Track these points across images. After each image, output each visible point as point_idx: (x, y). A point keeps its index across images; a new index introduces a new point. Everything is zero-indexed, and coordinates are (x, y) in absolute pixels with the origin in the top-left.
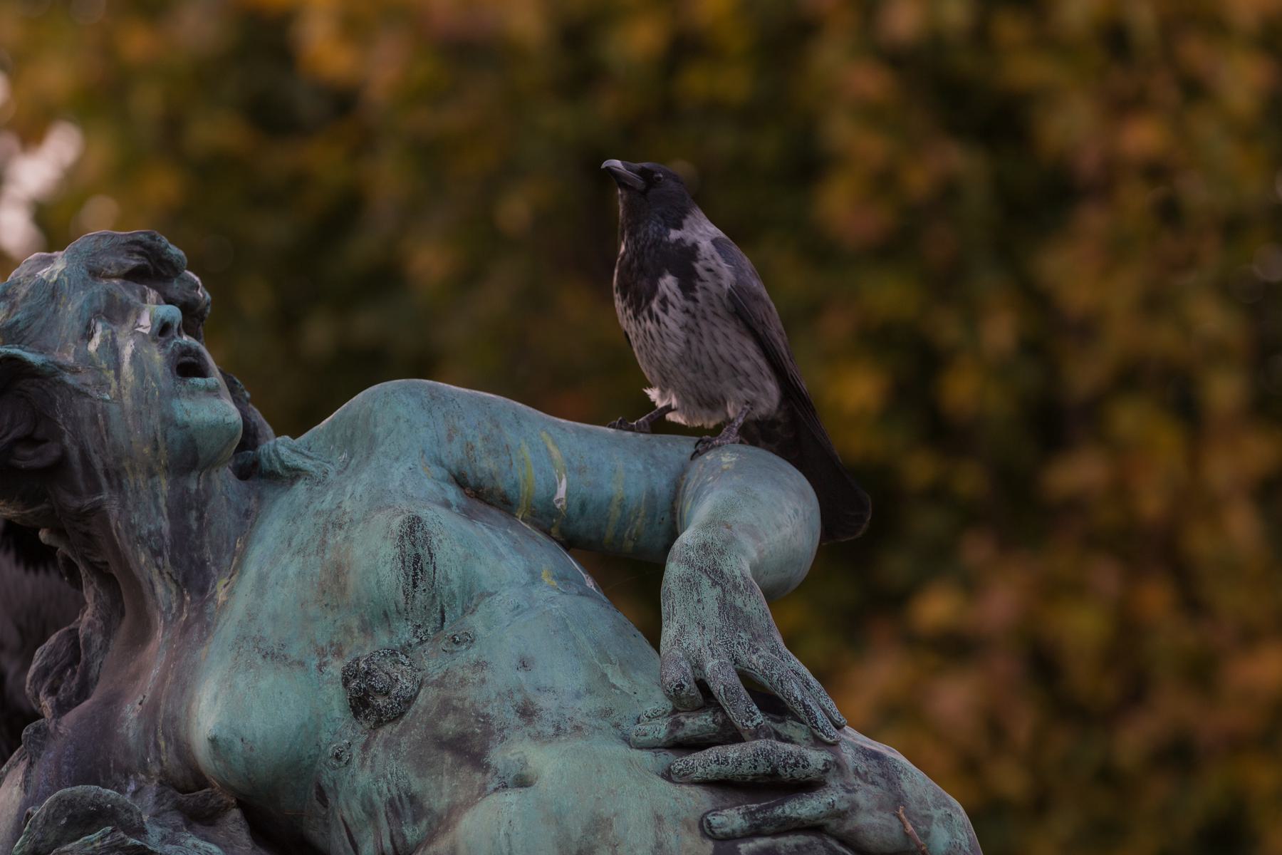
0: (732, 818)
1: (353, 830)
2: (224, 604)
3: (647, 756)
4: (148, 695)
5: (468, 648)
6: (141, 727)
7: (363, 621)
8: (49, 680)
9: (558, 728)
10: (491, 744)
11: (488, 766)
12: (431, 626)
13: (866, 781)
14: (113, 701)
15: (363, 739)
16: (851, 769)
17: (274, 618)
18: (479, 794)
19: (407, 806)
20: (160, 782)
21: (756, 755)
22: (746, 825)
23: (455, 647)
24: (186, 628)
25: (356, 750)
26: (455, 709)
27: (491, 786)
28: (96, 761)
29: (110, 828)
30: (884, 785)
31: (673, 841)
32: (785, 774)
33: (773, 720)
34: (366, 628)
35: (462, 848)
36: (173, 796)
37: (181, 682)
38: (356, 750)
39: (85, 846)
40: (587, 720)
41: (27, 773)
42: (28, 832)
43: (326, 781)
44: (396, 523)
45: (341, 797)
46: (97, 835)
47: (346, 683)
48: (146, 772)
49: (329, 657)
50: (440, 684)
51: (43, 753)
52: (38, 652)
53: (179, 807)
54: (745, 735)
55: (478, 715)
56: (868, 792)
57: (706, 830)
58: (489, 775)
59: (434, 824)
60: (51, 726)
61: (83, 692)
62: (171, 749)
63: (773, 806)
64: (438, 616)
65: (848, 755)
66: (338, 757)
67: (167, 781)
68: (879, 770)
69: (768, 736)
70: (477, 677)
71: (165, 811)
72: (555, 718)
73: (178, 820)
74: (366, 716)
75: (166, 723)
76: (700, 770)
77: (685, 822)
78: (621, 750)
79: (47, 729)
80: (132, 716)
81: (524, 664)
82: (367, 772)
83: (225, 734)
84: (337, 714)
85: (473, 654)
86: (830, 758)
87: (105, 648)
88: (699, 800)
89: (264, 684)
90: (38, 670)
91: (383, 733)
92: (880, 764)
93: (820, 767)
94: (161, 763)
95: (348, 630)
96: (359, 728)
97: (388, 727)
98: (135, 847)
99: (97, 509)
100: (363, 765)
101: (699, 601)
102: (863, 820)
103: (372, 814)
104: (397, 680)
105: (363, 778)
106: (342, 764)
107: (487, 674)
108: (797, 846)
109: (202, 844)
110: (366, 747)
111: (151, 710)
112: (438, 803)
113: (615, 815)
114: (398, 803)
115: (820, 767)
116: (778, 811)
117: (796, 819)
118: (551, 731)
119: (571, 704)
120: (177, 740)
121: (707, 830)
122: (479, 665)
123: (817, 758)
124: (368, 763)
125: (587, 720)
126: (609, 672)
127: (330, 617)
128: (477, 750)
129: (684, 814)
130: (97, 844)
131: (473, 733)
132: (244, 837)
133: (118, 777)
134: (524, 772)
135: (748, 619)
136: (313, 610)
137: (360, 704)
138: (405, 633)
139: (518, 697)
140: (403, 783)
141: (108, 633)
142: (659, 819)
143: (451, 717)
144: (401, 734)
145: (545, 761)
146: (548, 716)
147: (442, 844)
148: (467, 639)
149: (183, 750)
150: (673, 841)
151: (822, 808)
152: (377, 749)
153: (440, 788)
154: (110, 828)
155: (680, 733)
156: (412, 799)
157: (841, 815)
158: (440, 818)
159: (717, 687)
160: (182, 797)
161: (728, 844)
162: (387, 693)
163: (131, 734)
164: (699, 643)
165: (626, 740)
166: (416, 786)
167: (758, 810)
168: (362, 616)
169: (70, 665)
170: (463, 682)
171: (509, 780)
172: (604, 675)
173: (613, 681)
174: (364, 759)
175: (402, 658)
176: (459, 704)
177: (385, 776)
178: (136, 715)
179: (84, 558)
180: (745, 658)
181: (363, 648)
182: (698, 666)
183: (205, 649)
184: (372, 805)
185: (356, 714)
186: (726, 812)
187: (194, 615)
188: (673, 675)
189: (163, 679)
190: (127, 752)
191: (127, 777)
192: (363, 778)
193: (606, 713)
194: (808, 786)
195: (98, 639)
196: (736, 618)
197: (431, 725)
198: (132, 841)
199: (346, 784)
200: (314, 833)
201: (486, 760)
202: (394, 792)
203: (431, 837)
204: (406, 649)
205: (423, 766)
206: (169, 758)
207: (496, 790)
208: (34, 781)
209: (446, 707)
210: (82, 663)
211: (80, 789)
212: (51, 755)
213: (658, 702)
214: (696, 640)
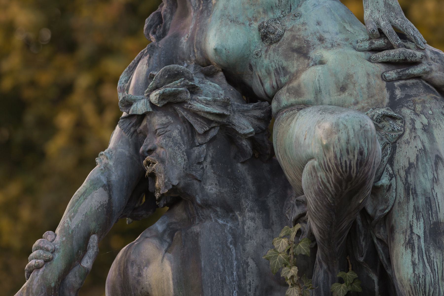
0: (392, 74)
1: (262, 79)
2: (215, 4)
3: (362, 54)
4: (190, 34)
5: (299, 18)
6: (188, 45)
7: (264, 9)
8: (152, 30)
9: (332, 45)
10: (310, 50)
11: (309, 57)
12: (287, 11)
13: (434, 61)
14: (177, 36)
15: (265, 48)
16: (430, 58)
17: (233, 8)
18: (307, 67)
19: (282, 71)
20: (195, 63)
21: (400, 53)
22: (397, 76)
23: (295, 18)
24: (202, 12)
25: (263, 52)
26: (297, 39)
27: (311, 64)
28: (172, 56)
29: (183, 79)
30: (440, 63)
31: (373, 82)
32: (409, 59)
33: (403, 41)
34: (265, 12)
35: (302, 85)
36: (200, 68)
37: (202, 29)
38: (263, 52)
39: (175, 85)
40: (341, 42)
41: (149, 60)
42: (155, 80)
43: (253, 62)
45: (258, 68)
46: (179, 81)
47: (259, 30)
48: (190, 60)
49: (253, 22)
50: (291, 30)
51: (154, 54)
52: (147, 20)
53: (202, 72)
54: (395, 47)
55: (305, 40)
56: (435, 65)
57: (383, 78)
58: (310, 60)
59: (291, 77)
60: (156, 45)
61: (164, 34)
62: (199, 52)
63: (405, 70)
64: (289, 8)
65: (429, 53)
66: (257, 55)
67: (197, 63)
68: (438, 58)
69: (402, 47)
70: (304, 28)
71: (197, 73)
72: (331, 41)
73: (202, 76)
74: (266, 41)
75: (197, 43)
76: (381, 58)
77: (377, 76)
78: (354, 52)
79: (154, 46)
80: (184, 41)
81: (318, 23)
82: (267, 60)
83: (219, 47)
84: (256, 40)
85: (302, 20)
86: (423, 54)
87: (171, 18)
88: (381, 68)
89: (232, 31)
90: (148, 26)
91: (273, 46)
92: (439, 56)
93: (420, 57)
94: (195, 57)
95: (259, 12)
96: (264, 45)
97: (274, 45)
98: (192, 85)
100: (266, 57)
101: (377, 2)
102: (434, 74)
103: (269, 73)
104: (277, 29)
105: (266, 62)
106: (258, 57)
107: (307, 27)
108: (413, 83)
109: (212, 84)
110: (267, 51)
111: (191, 39)
112: (293, 69)
113: (354, 73)
114: (278, 70)
115: (420, 57)
116: (407, 72)
117: (413, 74)
118: (330, 46)
119: (335, 37)
120: (201, 49)
121: (384, 78)
122: (304, 24)
123: (419, 54)
124: (268, 56)
125: (341, 42)
126: (346, 26)
127: (252, 8)
128: (305, 52)
129: (376, 73)
130: (179, 84)
131: (304, 46)
132: (224, 81)
133: (180, 61)
134: (322, 59)
135: (394, 8)
136: (247, 6)
137: (264, 37)
138: (278, 13)
139: (318, 34)
140: (280, 63)
141: (172, 13)
142: (368, 74)
143: (296, 41)
144: (279, 47)
145: (329, 56)
146: (328, 41)
147: (295, 84)
148: (300, 15)
149: (203, 52)
150: (373, 82)
151: (421, 71)
152: (271, 52)
153: (293, 65)
154: (183, 79)
155: (373, 46)
156: (284, 68)
157: (427, 73)
158: (293, 75)
159: (386, 31)
160: (203, 68)
161: (391, 83)
162: (274, 33)
163: (184, 47)
164: (378, 16)
165: (355, 48)
166: (285, 64)
167: (401, 71)
168: (263, 8)
169: (159, 24)
170: (299, 30)
171: (317, 62)
172: (345, 27)
173: (347, 29)
174: (266, 55)
175: (278, 22)
176: (299, 37)
177: (274, 61)
178: (186, 41)
180: (393, 21)
181: (266, 19)
182: (378, 24)
183: (209, 19)
184: (269, 70)
185: (263, 40)
186: (390, 72)
187: (204, 7)
188: (371, 26)
189: (194, 29)
190: (183, 53)
191: (183, 61)
192: (266, 62)
193: (347, 40)
194: (415, 63)
195: (168, 16)
196: (390, 8)
197: (289, 44)
198: (190, 83)
199: (260, 64)
200: (247, 80)
201: (308, 55)
202: (277, 66)
203: (290, 81)
204: (279, 19)
205: (287, 57)
206: (198, 55)
207: (313, 65)
208: (151, 63)
209: (294, 38)
210: (163, 24)
211: (172, 66)
212: (157, 54)
213: (363, 36)
214: (377, 15)
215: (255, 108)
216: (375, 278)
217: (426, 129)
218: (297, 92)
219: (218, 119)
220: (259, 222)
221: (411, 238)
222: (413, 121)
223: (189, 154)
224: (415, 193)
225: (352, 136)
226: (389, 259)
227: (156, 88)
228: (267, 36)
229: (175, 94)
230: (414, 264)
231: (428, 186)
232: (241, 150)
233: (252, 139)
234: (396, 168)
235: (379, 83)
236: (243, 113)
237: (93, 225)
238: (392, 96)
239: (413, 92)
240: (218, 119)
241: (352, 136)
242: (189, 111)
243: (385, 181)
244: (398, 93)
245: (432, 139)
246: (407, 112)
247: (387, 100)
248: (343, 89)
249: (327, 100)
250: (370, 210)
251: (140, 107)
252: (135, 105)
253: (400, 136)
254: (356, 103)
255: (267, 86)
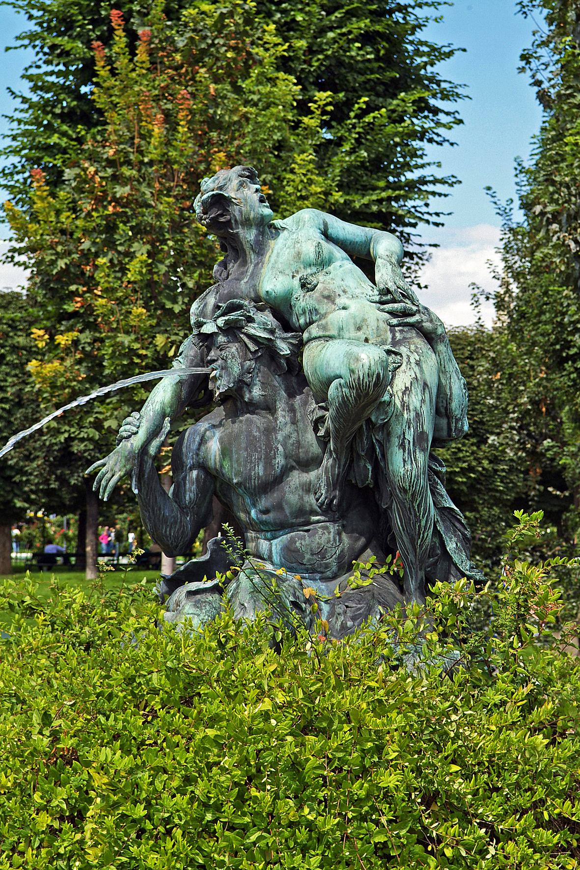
0: (395, 321)
44: (315, 244)
47: (300, 280)
57: (389, 324)
85: (331, 276)
99: (237, 233)
103: (304, 313)
112: (322, 311)
123: (415, 308)
136: (292, 262)
137: (303, 286)
147: (323, 322)
156: (316, 310)
179: (230, 244)
197: (322, 292)
200: (287, 316)
203: (320, 319)
209: (325, 289)
214: (386, 277)
215: (292, 337)
216: (370, 468)
217: (418, 363)
218: (325, 328)
219: (266, 342)
220: (288, 419)
221: (403, 442)
222: (408, 357)
223: (242, 367)
224: (408, 409)
225: (373, 364)
226: (384, 456)
227: (223, 315)
228: (304, 285)
229: (236, 321)
230: (404, 461)
231: (418, 406)
232: (279, 366)
233: (287, 358)
234: (395, 390)
235: (383, 326)
236: (284, 339)
237: (168, 410)
238: (394, 338)
239: (409, 335)
240: (266, 342)
241: (373, 364)
242: (245, 334)
243: (386, 398)
244: (398, 335)
245: (422, 371)
246: (403, 350)
247: (390, 340)
248: (359, 329)
249: (347, 335)
250: (373, 419)
251: (209, 328)
252: (205, 326)
253: (399, 367)
254: (366, 340)
255: (302, 321)
